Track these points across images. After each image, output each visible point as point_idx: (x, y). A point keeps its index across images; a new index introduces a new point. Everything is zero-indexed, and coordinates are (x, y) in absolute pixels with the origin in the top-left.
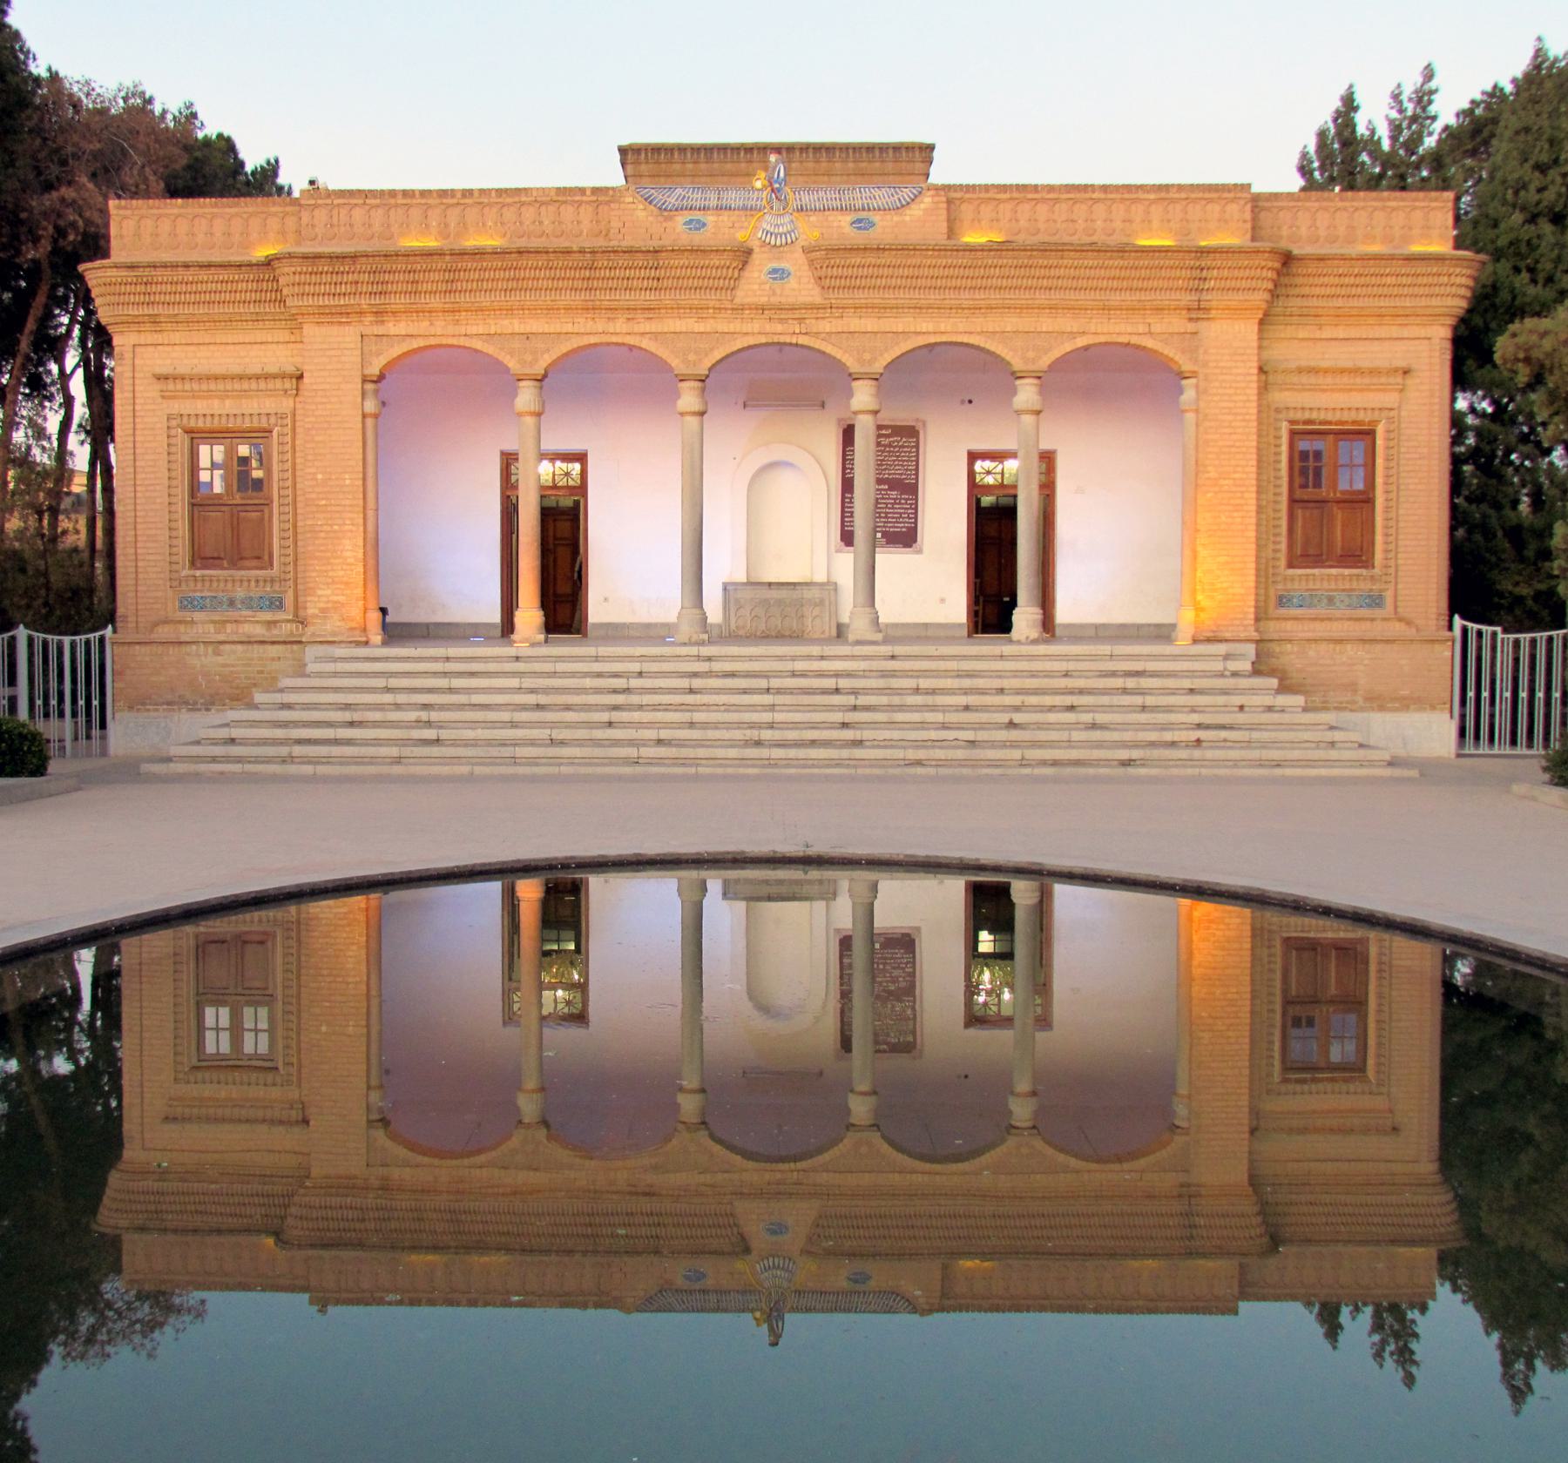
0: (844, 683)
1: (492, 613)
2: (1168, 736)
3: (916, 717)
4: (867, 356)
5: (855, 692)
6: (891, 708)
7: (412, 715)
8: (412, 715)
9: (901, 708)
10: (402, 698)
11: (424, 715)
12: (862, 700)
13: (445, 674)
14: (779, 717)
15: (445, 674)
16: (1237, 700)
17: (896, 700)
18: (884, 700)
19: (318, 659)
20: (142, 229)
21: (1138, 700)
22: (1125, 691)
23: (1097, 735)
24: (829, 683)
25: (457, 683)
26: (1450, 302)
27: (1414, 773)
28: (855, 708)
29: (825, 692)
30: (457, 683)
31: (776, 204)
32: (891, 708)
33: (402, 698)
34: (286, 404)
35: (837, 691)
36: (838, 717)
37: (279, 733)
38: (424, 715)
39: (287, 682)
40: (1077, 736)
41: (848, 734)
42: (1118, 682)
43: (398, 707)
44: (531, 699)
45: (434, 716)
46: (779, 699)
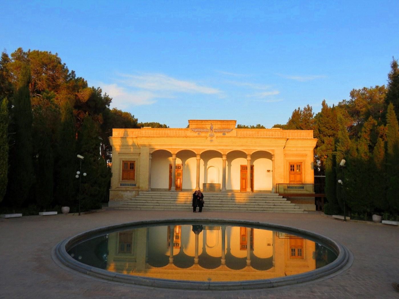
0: (220, 198)
1: (167, 187)
2: (269, 207)
3: (231, 203)
4: (225, 152)
5: (222, 199)
6: (227, 202)
7: (155, 202)
8: (155, 202)
9: (229, 202)
10: (154, 199)
11: (157, 202)
12: (223, 201)
13: (160, 196)
14: (211, 203)
15: (160, 196)
16: (280, 202)
17: (228, 201)
18: (226, 201)
19: (141, 193)
20: (117, 133)
21: (265, 201)
22: (263, 200)
23: (258, 206)
24: (218, 198)
25: (162, 197)
26: (313, 145)
27: (307, 212)
28: (222, 202)
29: (217, 199)
30: (162, 197)
31: (211, 131)
32: (227, 202)
33: (154, 199)
34: (138, 157)
35: (219, 199)
36: (219, 203)
37: (135, 204)
38: (157, 202)
39: (136, 197)
40: (256, 206)
41: (221, 206)
42: (262, 199)
43: (153, 200)
44: (173, 200)
45: (159, 202)
46: (211, 200)
